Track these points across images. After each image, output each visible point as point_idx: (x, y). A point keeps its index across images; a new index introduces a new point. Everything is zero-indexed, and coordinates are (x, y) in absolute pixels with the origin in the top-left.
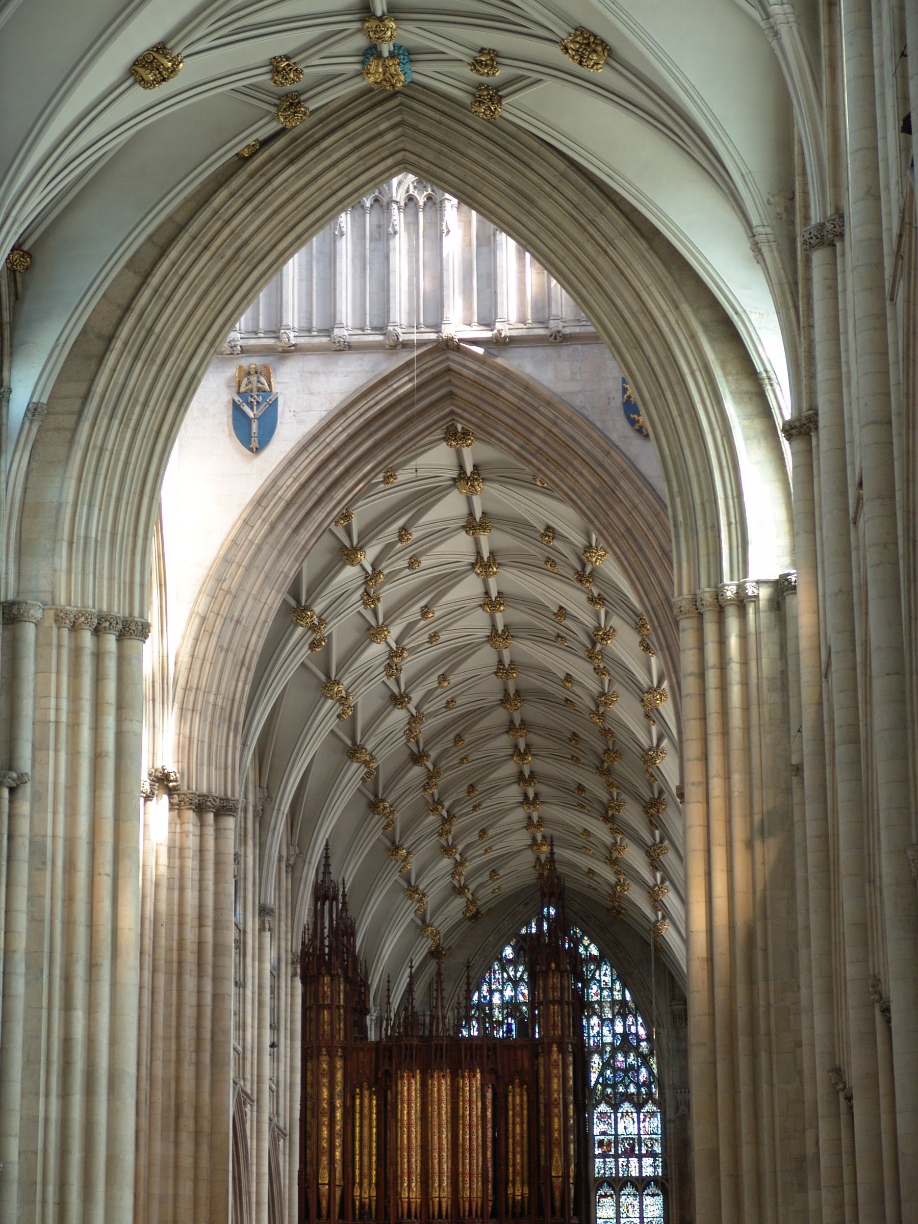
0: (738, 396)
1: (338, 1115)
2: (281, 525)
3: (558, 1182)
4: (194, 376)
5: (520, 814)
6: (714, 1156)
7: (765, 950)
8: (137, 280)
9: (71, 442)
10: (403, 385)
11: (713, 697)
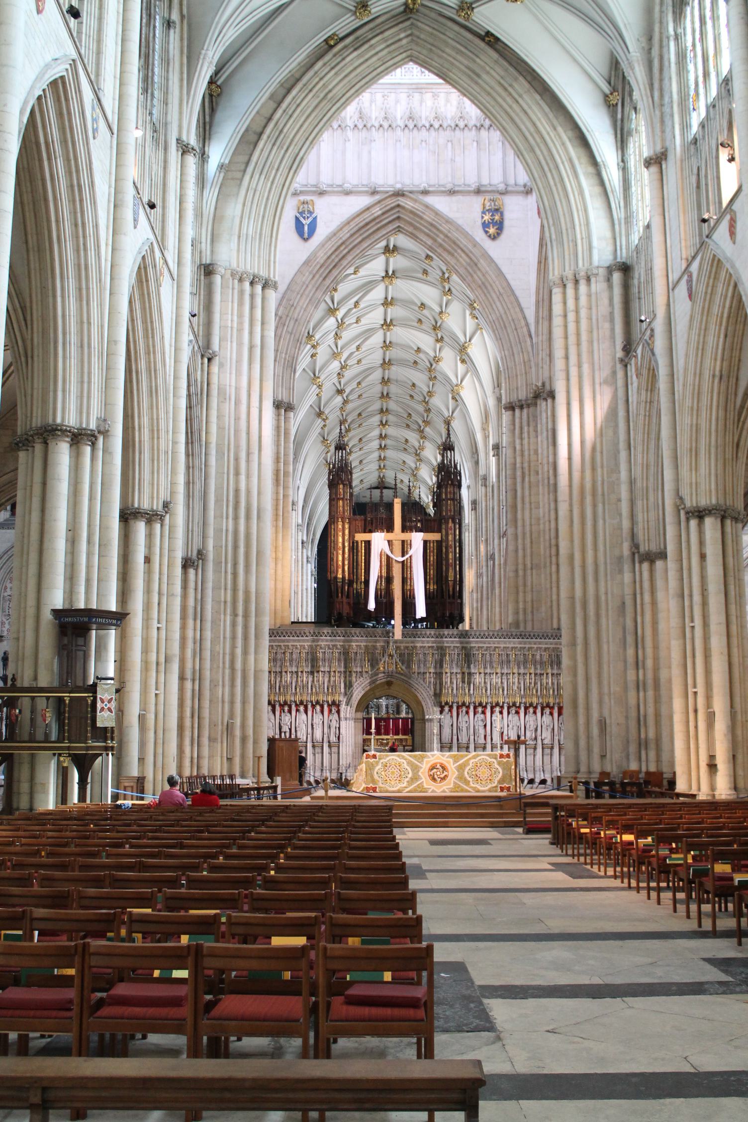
0: (586, 174)
1: (347, 550)
2: (317, 276)
3: (451, 583)
4: (302, 158)
5: (376, 455)
6: (571, 558)
7: (602, 453)
8: (275, 105)
9: (240, 185)
10: (377, 211)
11: (572, 327)
